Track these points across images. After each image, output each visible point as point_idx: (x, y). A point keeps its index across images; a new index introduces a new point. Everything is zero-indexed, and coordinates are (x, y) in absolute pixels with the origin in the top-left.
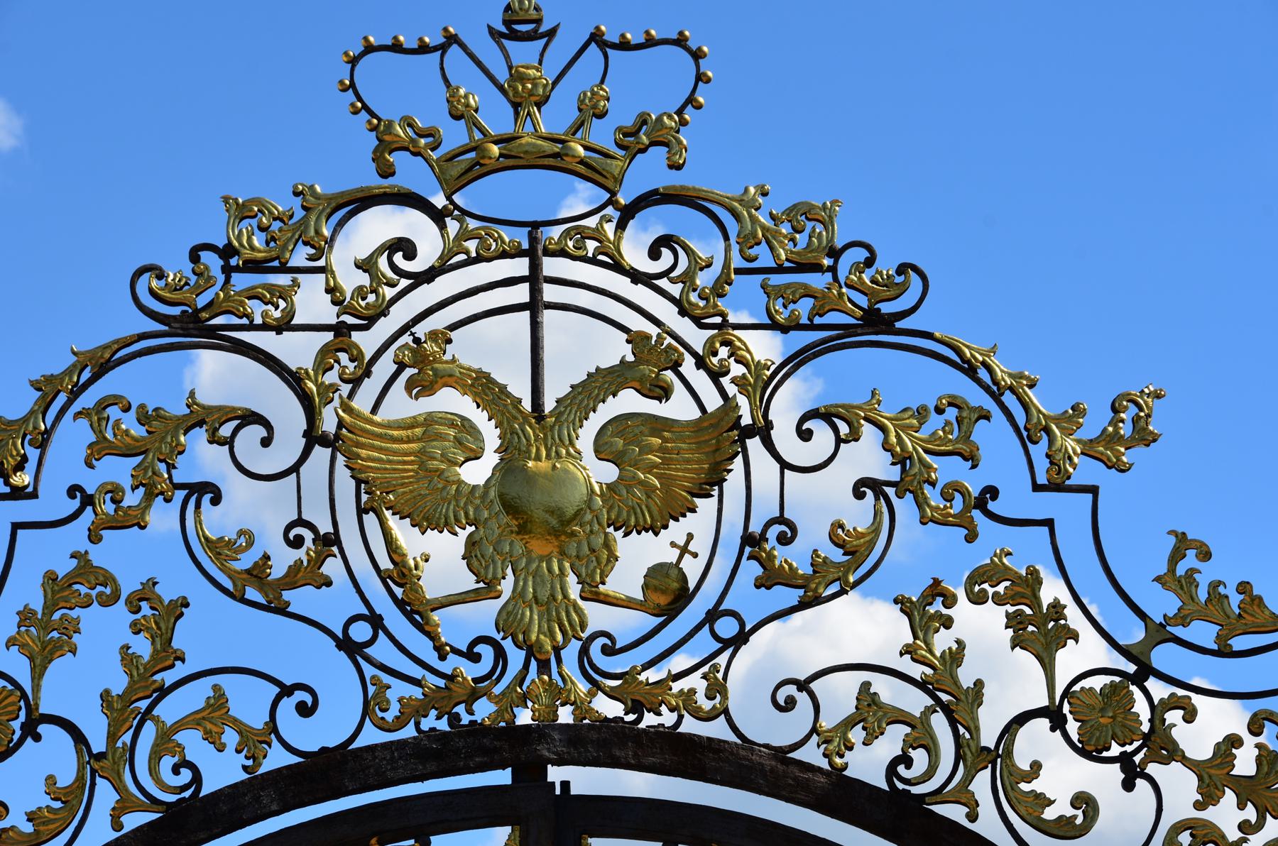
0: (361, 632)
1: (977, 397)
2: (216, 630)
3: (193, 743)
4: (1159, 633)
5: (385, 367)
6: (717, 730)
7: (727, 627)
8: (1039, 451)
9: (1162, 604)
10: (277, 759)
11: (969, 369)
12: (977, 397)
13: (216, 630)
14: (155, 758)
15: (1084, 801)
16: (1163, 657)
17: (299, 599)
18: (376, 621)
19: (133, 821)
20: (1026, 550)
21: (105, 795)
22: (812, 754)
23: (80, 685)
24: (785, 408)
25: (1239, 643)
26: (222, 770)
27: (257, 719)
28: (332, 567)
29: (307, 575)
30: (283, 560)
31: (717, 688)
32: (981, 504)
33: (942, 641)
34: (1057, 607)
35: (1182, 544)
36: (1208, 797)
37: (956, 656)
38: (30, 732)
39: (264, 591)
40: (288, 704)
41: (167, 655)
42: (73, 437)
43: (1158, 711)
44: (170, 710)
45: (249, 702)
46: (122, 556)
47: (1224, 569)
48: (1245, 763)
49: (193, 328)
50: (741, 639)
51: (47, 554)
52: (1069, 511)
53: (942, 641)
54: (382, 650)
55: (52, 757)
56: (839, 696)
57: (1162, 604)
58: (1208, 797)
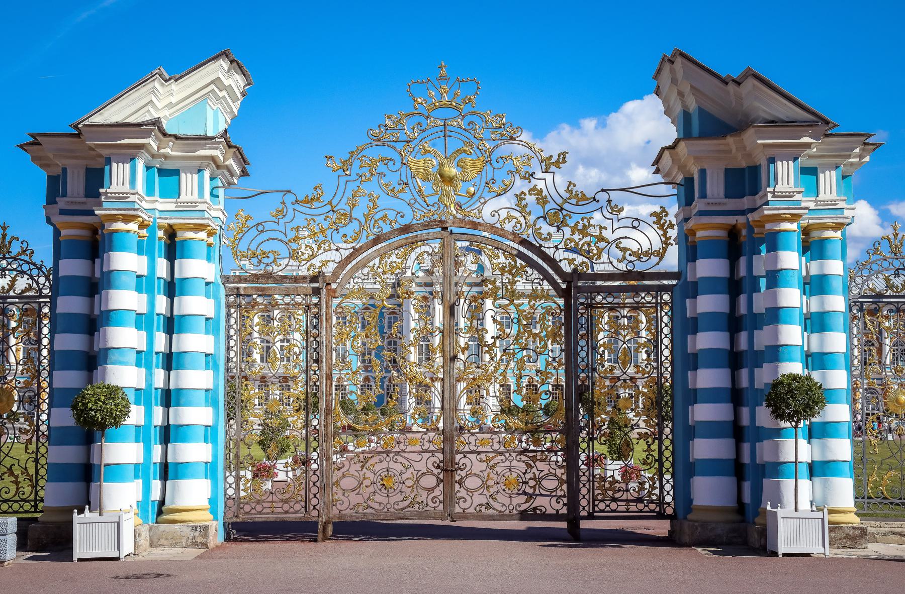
0: (412, 202)
1: (531, 154)
2: (385, 202)
3: (381, 223)
4: (565, 201)
5: (416, 149)
6: (480, 221)
7: (482, 201)
8: (543, 165)
9: (566, 195)
10: (396, 226)
11: (530, 148)
12: (531, 154)
13: (385, 202)
14: (374, 226)
15: (549, 234)
16: (566, 206)
17: (401, 195)
18: (415, 200)
19: (370, 238)
20: (540, 185)
21: (365, 234)
22: (498, 225)
23: (358, 213)
24: (494, 157)
25: (580, 203)
26: (386, 229)
27: (393, 218)
28: (407, 190)
29: (401, 191)
30: (398, 188)
31: (480, 213)
32: (532, 175)
33: (523, 203)
34: (546, 196)
35: (570, 183)
36: (573, 233)
37: (526, 206)
38: (351, 221)
39: (393, 193)
40: (399, 216)
41: (375, 206)
42: (357, 163)
43: (564, 217)
44: (376, 217)
45: (391, 215)
46: (366, 188)
47: (579, 188)
48: (580, 227)
49: (379, 141)
50: (485, 202)
51: (352, 186)
52: (549, 177)
53: (523, 203)
54: (417, 206)
55: (355, 226)
56: (503, 214)
57: (566, 195)
58: (573, 233)
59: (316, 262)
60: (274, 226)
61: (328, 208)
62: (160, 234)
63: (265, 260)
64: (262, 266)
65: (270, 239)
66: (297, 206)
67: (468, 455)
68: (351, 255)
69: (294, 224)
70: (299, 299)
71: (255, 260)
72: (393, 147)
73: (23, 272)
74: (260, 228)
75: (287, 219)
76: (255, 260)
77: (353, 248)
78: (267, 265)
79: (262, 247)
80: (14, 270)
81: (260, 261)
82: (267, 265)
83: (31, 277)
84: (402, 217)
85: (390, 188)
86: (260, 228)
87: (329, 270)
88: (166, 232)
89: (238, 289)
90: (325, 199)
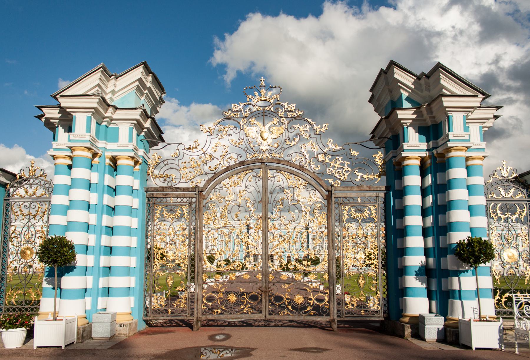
0: (246, 149)
6: (282, 159)
7: (283, 149)
10: (237, 162)
18: (247, 148)
26: (232, 163)
28: (243, 143)
50: (285, 150)
54: (248, 151)
59: (195, 181)
60: (173, 161)
61: (202, 152)
62: (108, 161)
63: (168, 179)
64: (167, 182)
65: (170, 168)
66: (185, 151)
67: (276, 284)
68: (213, 176)
69: (183, 161)
70: (185, 200)
71: (162, 180)
72: (236, 121)
73: (41, 185)
74: (165, 162)
75: (180, 158)
76: (162, 180)
77: (214, 173)
78: (169, 182)
79: (165, 173)
80: (36, 184)
81: (165, 180)
82: (169, 182)
83: (45, 188)
84: (241, 157)
85: (234, 142)
86: (165, 162)
87: (201, 185)
88: (110, 160)
89: (153, 194)
90: (199, 148)
